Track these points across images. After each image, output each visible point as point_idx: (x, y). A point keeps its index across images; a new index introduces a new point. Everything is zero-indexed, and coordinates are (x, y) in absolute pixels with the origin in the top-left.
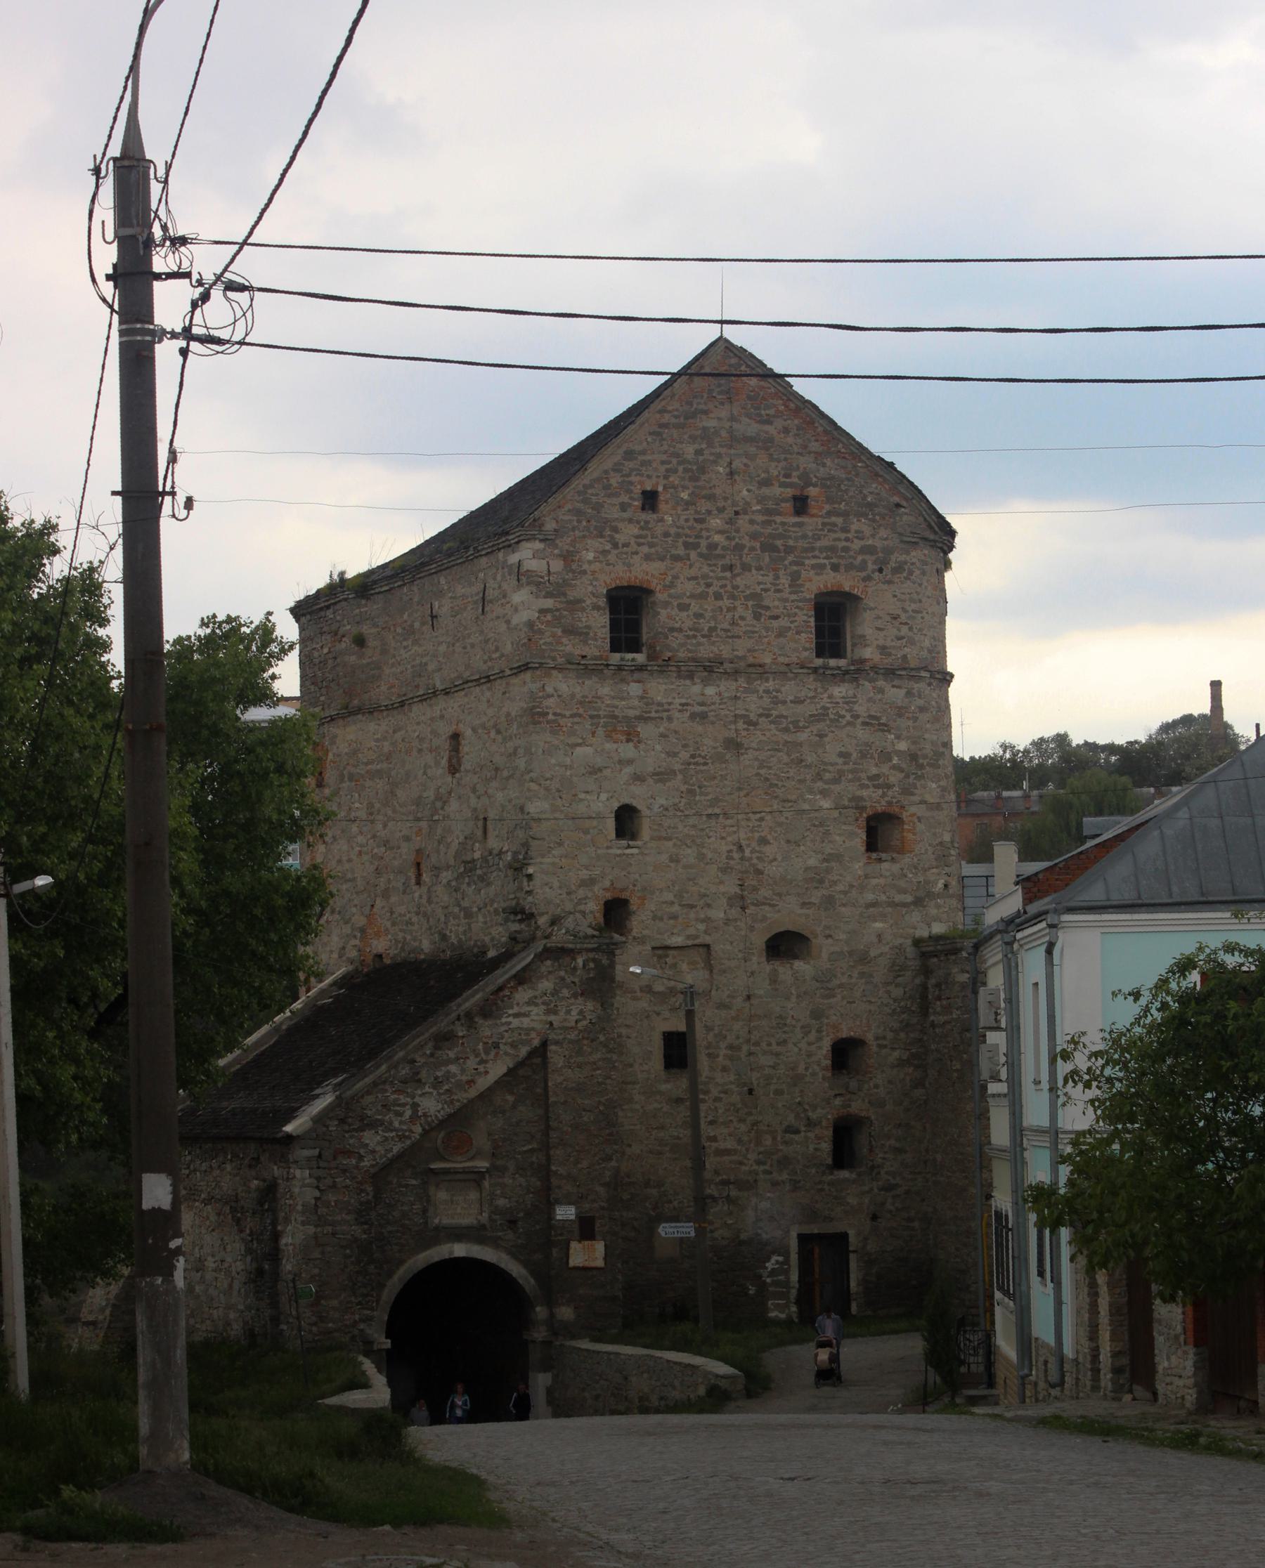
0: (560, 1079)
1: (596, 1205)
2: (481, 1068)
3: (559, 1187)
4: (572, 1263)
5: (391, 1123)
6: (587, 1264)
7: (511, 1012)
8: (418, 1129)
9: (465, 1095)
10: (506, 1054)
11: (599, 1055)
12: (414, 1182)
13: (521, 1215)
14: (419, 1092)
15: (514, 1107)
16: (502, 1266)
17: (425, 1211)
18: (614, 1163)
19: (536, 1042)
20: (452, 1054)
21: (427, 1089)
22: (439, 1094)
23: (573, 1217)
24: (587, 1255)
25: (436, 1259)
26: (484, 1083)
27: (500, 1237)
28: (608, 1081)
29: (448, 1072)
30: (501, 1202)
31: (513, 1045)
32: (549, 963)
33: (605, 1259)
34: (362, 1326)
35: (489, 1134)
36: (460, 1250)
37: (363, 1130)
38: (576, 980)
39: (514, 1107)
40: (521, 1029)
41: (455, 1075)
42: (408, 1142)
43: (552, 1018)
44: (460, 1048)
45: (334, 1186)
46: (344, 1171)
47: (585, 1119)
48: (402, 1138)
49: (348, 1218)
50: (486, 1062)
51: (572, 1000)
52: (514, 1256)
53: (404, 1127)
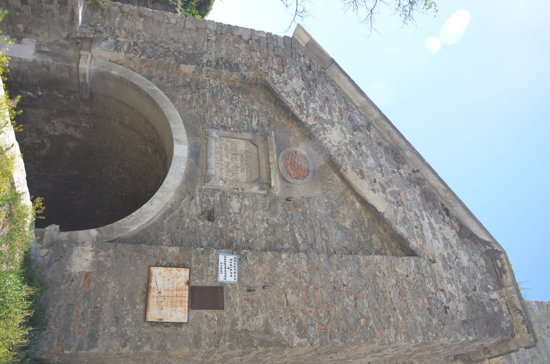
0: (383, 268)
1: (239, 312)
2: (377, 186)
3: (261, 261)
4: (155, 271)
5: (314, 101)
6: (153, 293)
7: (432, 220)
8: (310, 121)
9: (349, 167)
10: (396, 212)
11: (419, 318)
12: (254, 123)
13: (221, 226)
14: (344, 129)
15: (340, 227)
16: (158, 194)
17: (225, 128)
18: (297, 340)
19: (414, 244)
20: (383, 161)
21: (348, 136)
22: (346, 145)
23: (221, 278)
24: (168, 291)
25: (173, 126)
26: (363, 187)
27: (193, 198)
28: (393, 331)
29: (367, 157)
30: (235, 205)
31: (405, 221)
32: (483, 263)
33: (160, 323)
34: (111, 40)
35: (308, 199)
36: (181, 151)
37: (303, 79)
38: (478, 292)
39: (340, 227)
40: (422, 230)
41: (366, 162)
42: (297, 112)
43: (440, 263)
44: (390, 170)
45: (251, 50)
46: (266, 59)
47: (347, 300)
48: (300, 106)
49: (223, 52)
50: (384, 191)
51: (460, 287)
52: (169, 212)
53: (311, 111)
